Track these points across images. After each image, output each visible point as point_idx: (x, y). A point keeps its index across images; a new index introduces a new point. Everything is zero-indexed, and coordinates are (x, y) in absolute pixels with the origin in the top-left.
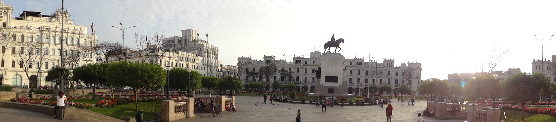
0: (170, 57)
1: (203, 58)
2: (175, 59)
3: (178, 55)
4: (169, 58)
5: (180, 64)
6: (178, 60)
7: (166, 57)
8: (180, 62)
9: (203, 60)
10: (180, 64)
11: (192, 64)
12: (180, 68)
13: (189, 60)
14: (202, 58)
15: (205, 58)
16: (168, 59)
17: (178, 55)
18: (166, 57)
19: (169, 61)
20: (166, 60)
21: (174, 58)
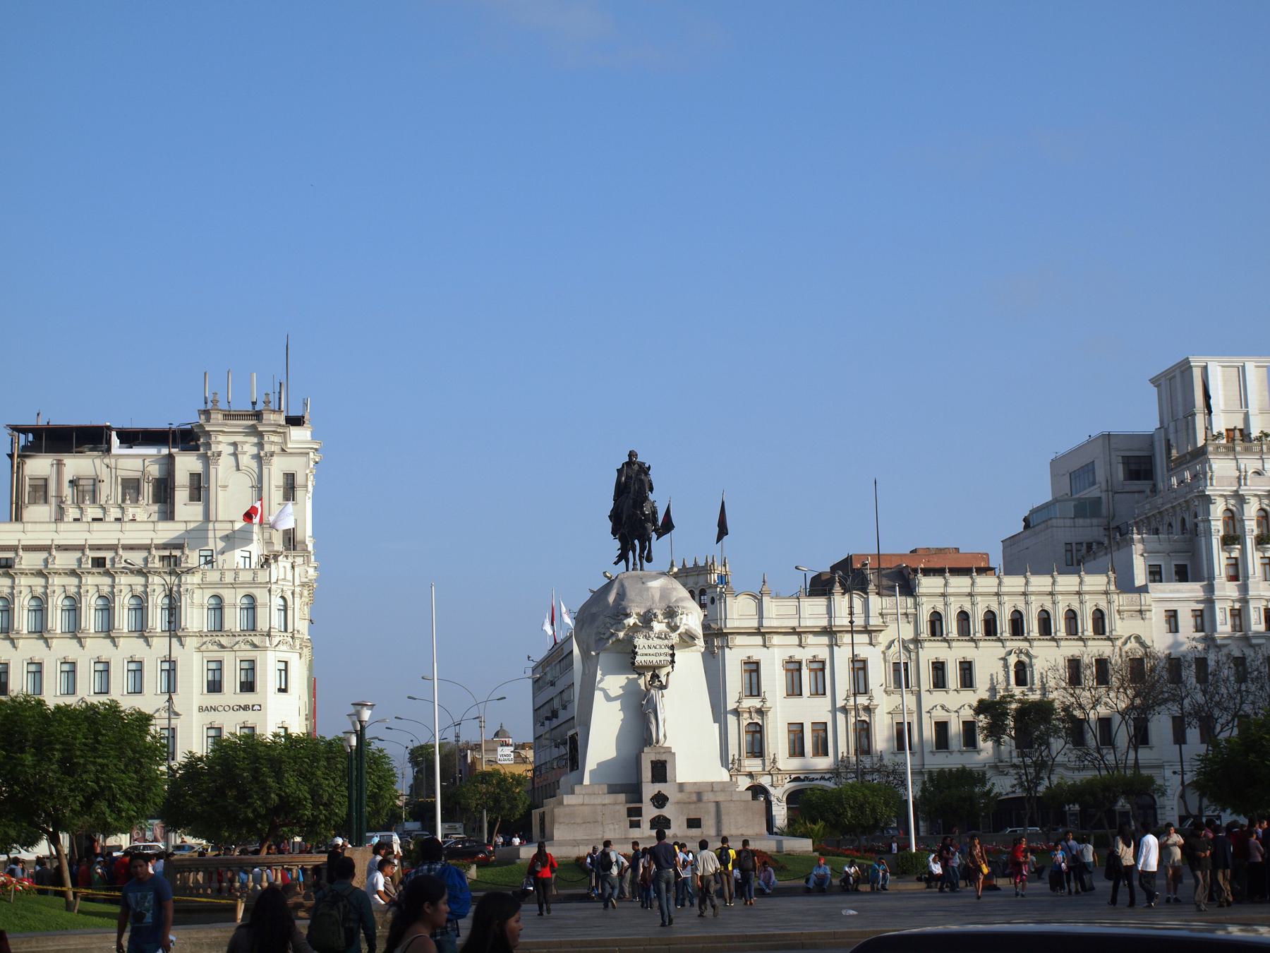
0: (829, 631)
1: (1210, 589)
2: (883, 639)
3: (916, 605)
4: (825, 640)
5: (939, 667)
6: (917, 641)
7: (794, 632)
8: (932, 651)
9: (1210, 602)
10: (939, 667)
11: (1072, 648)
12: (939, 697)
13: (1033, 627)
14: (1192, 590)
15: (1226, 591)
16: (817, 647)
17: (916, 605)
18: (794, 632)
19: (823, 654)
20: (803, 655)
21: (867, 630)
